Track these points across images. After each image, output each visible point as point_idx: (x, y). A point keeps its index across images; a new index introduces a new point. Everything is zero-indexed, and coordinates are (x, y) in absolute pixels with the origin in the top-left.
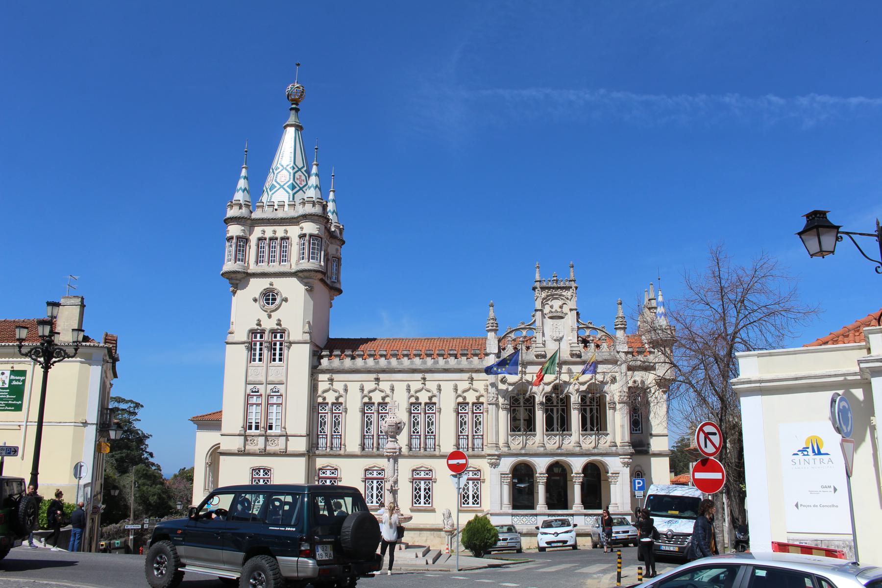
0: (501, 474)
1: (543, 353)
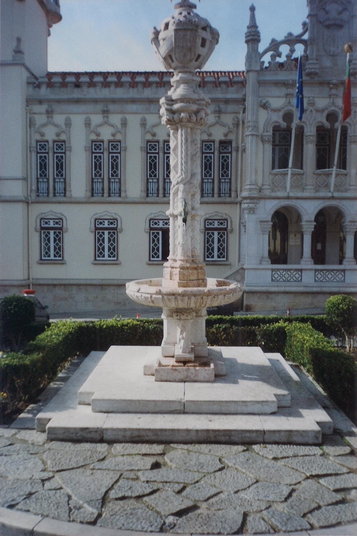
0: (261, 222)
1: (317, 71)
